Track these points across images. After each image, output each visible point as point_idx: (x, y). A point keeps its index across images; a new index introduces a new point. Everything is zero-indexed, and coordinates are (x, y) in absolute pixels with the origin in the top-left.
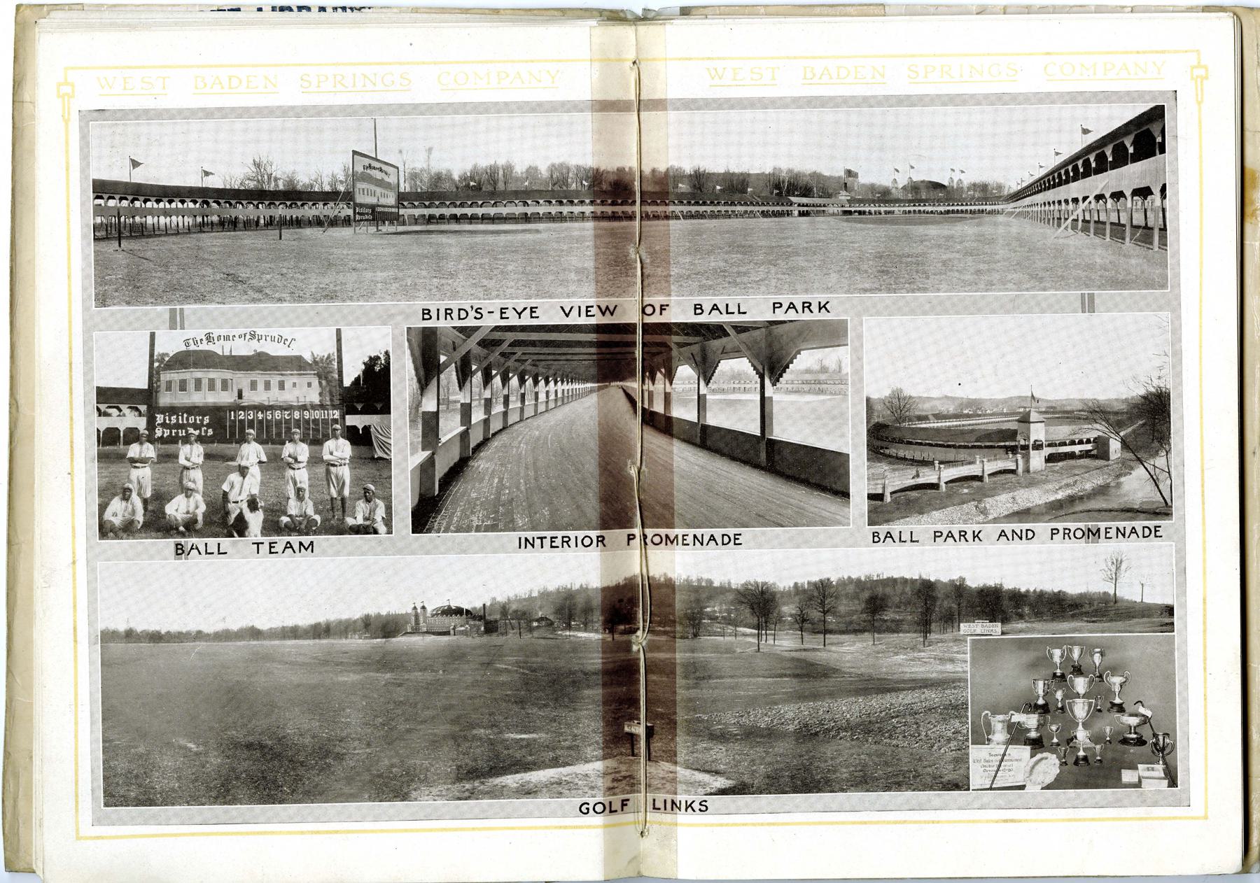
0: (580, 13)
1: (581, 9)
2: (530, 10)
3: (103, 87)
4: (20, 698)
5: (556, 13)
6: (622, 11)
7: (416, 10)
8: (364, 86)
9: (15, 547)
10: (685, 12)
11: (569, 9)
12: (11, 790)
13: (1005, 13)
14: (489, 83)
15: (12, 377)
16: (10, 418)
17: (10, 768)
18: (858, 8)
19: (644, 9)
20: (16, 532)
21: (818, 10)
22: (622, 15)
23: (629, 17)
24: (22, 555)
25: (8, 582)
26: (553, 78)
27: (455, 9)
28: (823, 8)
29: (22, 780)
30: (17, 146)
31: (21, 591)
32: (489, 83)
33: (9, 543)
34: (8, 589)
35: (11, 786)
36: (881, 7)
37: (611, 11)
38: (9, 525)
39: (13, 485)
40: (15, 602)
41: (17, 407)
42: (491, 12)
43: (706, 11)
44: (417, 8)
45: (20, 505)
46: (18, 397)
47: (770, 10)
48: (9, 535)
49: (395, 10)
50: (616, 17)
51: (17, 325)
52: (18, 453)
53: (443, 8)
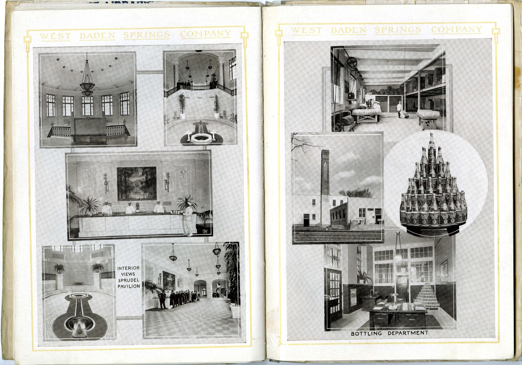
3: (294, 32)
14: (452, 32)
26: (479, 29)
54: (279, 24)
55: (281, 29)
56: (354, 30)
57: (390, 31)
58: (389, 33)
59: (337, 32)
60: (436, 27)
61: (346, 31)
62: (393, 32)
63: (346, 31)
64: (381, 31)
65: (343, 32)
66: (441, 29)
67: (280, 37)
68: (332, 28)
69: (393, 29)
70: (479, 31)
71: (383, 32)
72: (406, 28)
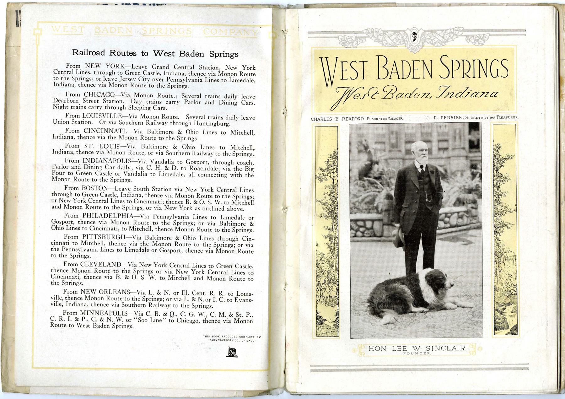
1: (260, 5)
2: (237, 5)
4: (9, 314)
5: (249, 6)
6: (279, 5)
7: (186, 5)
10: (306, 6)
12: (5, 355)
13: (450, 6)
15: (5, 170)
16: (4, 188)
17: (4, 346)
18: (384, 4)
19: (288, 5)
22: (278, 7)
24: (10, 250)
25: (3, 262)
27: (204, 5)
29: (10, 352)
31: (9, 266)
33: (4, 244)
34: (3, 265)
35: (5, 353)
36: (395, 4)
37: (274, 5)
38: (4, 236)
39: (6, 218)
41: (8, 183)
42: (220, 6)
43: (316, 6)
44: (187, 4)
45: (9, 228)
47: (344, 5)
48: (4, 241)
49: (177, 5)
50: (276, 7)
52: (8, 204)
53: (198, 4)
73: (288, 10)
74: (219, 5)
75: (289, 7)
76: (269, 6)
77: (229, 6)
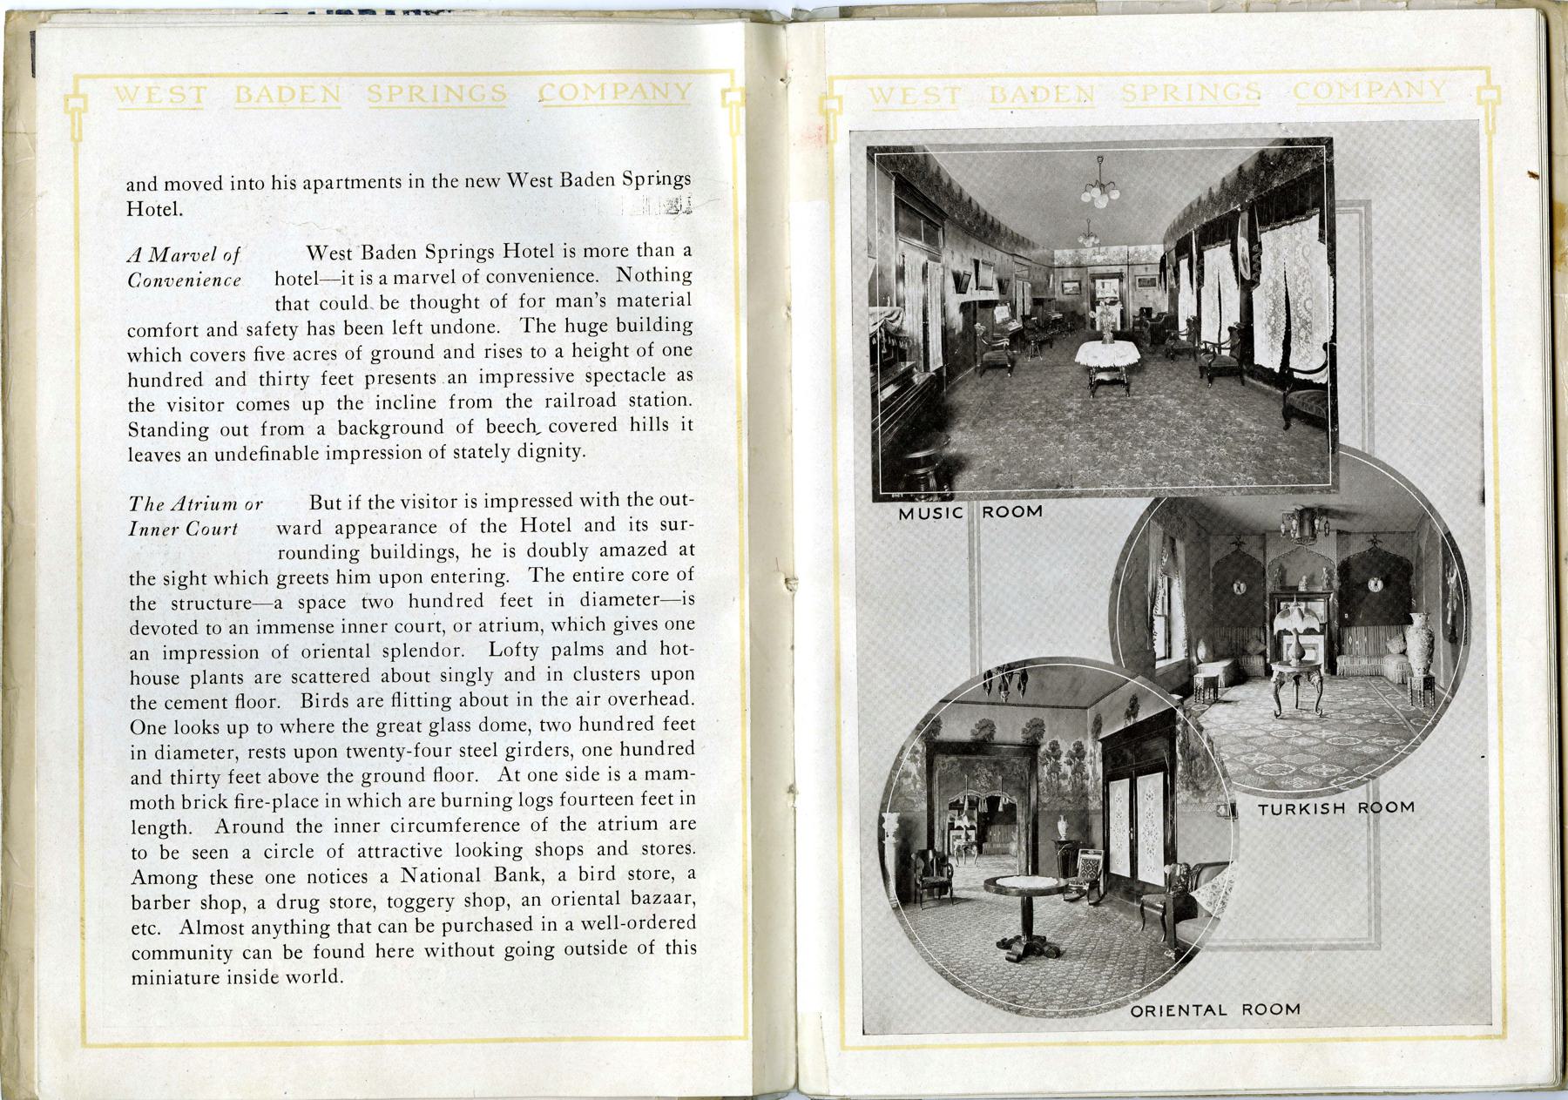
0: (713, 14)
1: (715, 10)
2: (651, 11)
5: (684, 15)
6: (766, 11)
8: (448, 101)
9: (11, 693)
10: (846, 13)
11: (701, 10)
13: (1247, 11)
20: (12, 672)
21: (1013, 9)
22: (766, 16)
23: (775, 18)
28: (1018, 7)
30: (8, 188)
32: (603, 98)
37: (753, 12)
40: (12, 761)
43: (872, 12)
46: (13, 504)
50: (760, 18)
51: (11, 412)
53: (542, 11)
54: (77, 78)
55: (82, 90)
56: (304, 93)
57: (414, 97)
58: (411, 104)
59: (252, 101)
60: (553, 85)
61: (280, 97)
62: (423, 100)
63: (280, 97)
64: (386, 97)
65: (271, 101)
66: (568, 92)
67: (80, 114)
68: (239, 88)
69: (422, 90)
70: (683, 98)
71: (391, 100)
72: (461, 87)
73: (791, 27)
74: (600, 11)
75: (798, 16)
76: (740, 14)
77: (628, 14)
